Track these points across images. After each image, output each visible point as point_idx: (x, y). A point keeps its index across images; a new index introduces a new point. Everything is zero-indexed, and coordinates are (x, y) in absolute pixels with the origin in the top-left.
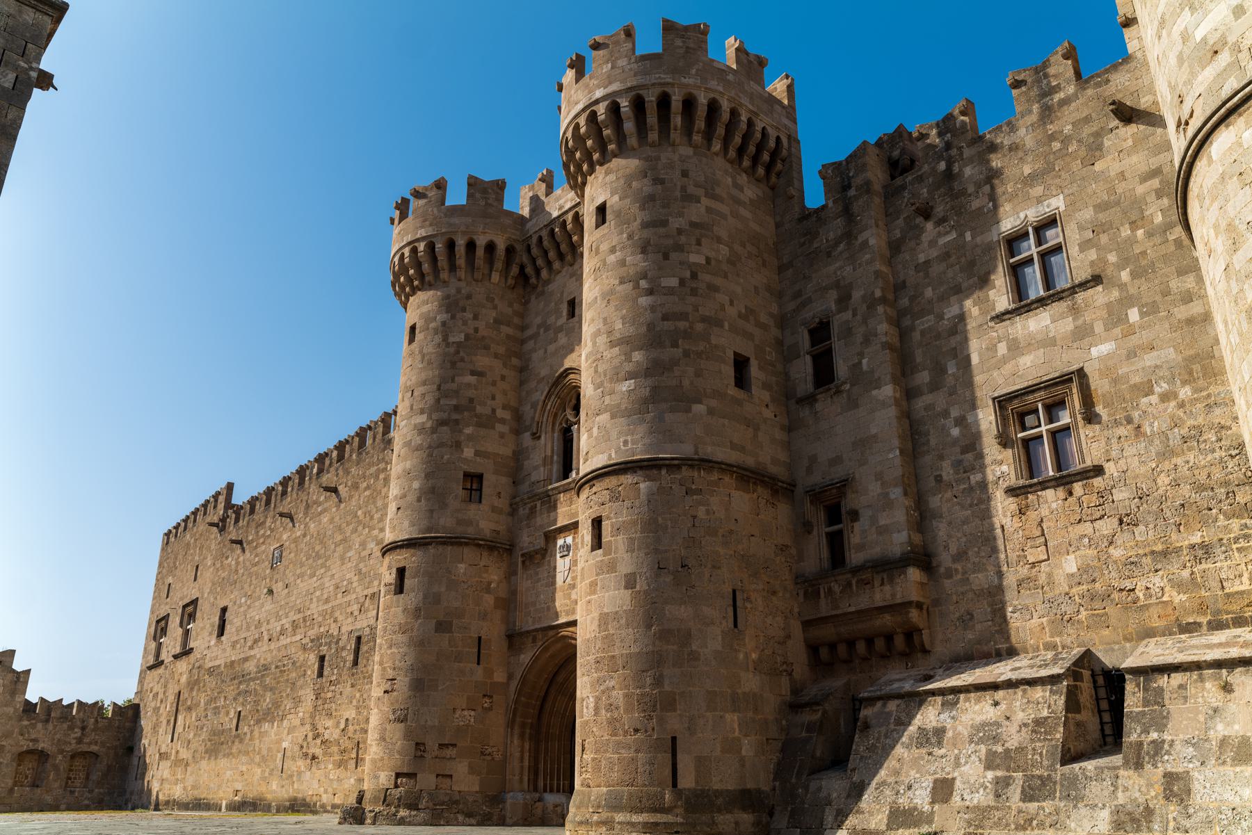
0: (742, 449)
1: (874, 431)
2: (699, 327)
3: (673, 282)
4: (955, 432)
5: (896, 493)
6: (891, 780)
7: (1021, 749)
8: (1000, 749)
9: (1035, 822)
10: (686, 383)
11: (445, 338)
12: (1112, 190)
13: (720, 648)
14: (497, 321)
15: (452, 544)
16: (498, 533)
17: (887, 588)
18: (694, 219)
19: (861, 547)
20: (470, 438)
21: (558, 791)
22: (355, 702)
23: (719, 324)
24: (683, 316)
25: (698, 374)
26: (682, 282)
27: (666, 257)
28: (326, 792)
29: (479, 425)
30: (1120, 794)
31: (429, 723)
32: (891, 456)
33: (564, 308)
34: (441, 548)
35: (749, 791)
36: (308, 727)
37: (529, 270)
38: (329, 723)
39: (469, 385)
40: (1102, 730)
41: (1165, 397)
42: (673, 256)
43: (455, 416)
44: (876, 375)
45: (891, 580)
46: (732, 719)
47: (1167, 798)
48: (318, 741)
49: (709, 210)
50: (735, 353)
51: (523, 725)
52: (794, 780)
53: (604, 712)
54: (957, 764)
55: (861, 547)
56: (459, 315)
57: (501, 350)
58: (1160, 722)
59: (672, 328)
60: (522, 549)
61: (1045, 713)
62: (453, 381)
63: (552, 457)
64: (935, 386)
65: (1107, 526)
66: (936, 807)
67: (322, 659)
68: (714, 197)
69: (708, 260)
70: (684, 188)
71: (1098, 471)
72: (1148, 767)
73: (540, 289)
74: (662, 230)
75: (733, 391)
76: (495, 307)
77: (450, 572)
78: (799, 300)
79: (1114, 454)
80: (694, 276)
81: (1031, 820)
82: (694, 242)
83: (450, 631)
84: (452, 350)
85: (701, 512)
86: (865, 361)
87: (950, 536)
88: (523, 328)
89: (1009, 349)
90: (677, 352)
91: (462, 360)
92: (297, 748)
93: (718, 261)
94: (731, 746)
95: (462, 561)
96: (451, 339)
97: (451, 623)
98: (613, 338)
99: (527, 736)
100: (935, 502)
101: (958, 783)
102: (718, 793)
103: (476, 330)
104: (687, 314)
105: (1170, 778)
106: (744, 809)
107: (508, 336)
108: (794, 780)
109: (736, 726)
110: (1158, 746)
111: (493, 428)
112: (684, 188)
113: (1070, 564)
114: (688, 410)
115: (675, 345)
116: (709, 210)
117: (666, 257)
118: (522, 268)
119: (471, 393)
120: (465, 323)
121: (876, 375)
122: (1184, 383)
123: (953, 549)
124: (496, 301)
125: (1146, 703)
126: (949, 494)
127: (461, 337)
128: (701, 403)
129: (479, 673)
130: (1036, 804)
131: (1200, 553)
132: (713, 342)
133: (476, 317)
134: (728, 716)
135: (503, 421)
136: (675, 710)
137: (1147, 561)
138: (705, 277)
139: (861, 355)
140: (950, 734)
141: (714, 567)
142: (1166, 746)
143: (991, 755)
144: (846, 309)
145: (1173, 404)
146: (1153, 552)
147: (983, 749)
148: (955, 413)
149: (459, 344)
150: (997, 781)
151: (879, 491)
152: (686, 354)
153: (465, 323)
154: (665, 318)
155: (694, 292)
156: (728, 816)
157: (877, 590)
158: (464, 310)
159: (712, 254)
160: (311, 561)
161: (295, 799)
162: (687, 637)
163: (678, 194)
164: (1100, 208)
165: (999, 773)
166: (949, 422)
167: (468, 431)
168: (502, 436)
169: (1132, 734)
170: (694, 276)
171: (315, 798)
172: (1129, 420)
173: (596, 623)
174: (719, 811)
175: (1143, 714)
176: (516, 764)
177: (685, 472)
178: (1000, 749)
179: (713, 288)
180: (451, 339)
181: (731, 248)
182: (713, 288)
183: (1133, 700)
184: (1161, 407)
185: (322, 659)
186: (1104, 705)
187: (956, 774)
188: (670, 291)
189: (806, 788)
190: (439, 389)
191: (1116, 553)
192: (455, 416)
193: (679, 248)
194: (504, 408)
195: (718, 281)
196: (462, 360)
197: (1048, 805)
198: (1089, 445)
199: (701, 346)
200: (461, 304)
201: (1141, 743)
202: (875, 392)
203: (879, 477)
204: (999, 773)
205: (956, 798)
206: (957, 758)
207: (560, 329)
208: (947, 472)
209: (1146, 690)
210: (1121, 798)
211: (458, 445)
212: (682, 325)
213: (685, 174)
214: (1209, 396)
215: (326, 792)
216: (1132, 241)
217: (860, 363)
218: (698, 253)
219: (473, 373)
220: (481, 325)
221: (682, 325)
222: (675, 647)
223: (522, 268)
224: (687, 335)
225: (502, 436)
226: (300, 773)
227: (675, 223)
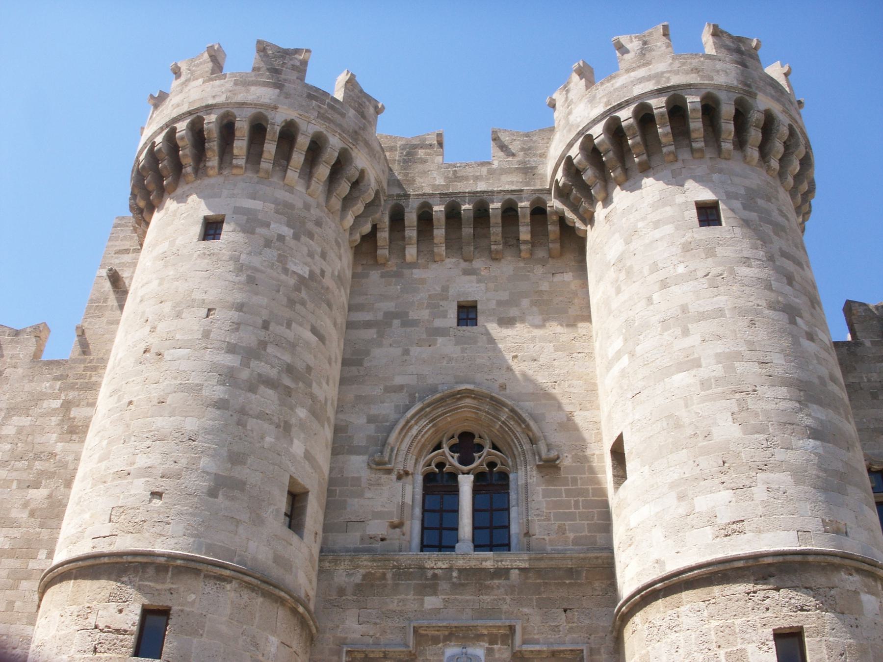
15: (265, 594)
34: (246, 595)
37: (383, 236)
43: (287, 381)
60: (343, 642)
62: (289, 326)
63: (413, 507)
77: (256, 645)
84: (292, 281)
91: (303, 303)
95: (274, 632)
127: (305, 272)
149: (302, 280)
153: (311, 255)
180: (292, 267)
190: (266, 326)
192: (287, 381)
207: (443, 332)
211: (286, 428)
219: (314, 331)
223: (375, 228)
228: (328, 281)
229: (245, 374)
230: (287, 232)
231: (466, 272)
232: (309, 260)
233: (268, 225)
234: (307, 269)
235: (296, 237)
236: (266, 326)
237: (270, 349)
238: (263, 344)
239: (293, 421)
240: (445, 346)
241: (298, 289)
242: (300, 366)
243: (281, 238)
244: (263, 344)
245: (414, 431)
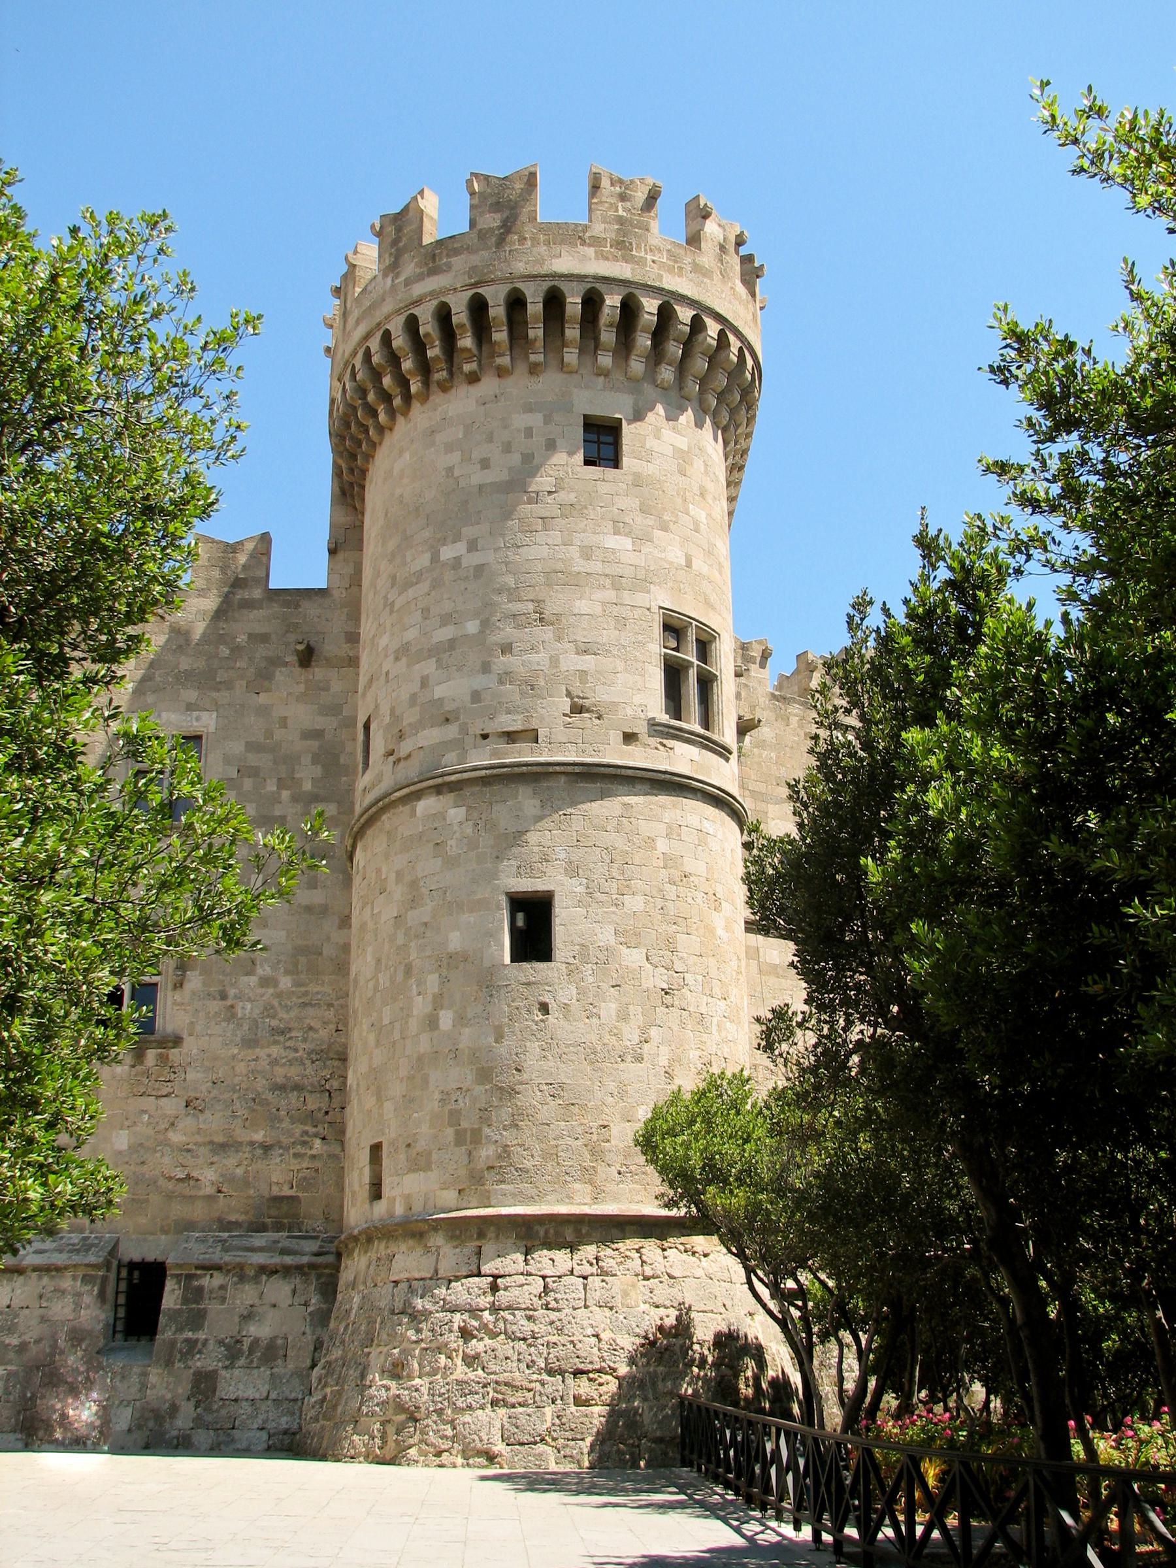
12: (269, 734)
40: (114, 1326)
41: (265, 982)
58: (197, 1320)
65: (171, 1106)
71: (177, 1041)
79: (198, 1028)
110: (191, 1344)
113: (122, 1140)
122: (287, 972)
125: (185, 1300)
131: (259, 1152)
137: (204, 1151)
142: (199, 1345)
145: (271, 991)
146: (211, 1142)
164: (251, 747)
169: (166, 1332)
172: (223, 996)
183: (171, 1297)
184: (261, 991)
186: (122, 1300)
191: (176, 1137)
198: (172, 1012)
209: (186, 1288)
214: (306, 993)
216: (275, 799)
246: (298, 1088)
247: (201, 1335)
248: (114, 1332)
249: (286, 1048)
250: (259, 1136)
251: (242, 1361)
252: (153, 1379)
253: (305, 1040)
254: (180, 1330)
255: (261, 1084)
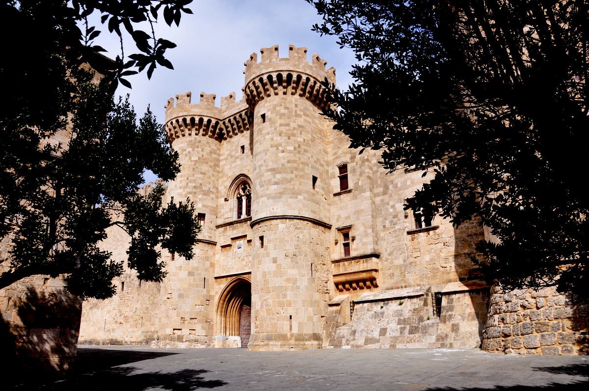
0: (314, 212)
1: (362, 208)
2: (301, 166)
3: (292, 148)
4: (391, 210)
5: (370, 231)
6: (366, 329)
7: (409, 318)
8: (402, 318)
9: (412, 341)
10: (296, 187)
11: (190, 158)
13: (307, 285)
14: (211, 152)
16: (211, 237)
17: (365, 264)
18: (299, 124)
19: (356, 250)
20: (200, 199)
21: (235, 335)
22: (139, 301)
23: (307, 165)
24: (295, 161)
25: (300, 184)
26: (295, 148)
27: (289, 138)
28: (127, 336)
29: (204, 194)
30: (439, 331)
31: (186, 310)
32: (368, 217)
33: (240, 149)
35: (316, 334)
36: (117, 311)
37: (224, 131)
38: (128, 309)
39: (199, 178)
42: (291, 138)
43: (194, 190)
44: (364, 188)
45: (367, 262)
46: (310, 309)
47: (452, 331)
48: (122, 317)
49: (305, 121)
50: (313, 176)
51: (221, 312)
52: (330, 330)
53: (265, 307)
54: (388, 323)
55: (356, 250)
56: (195, 149)
57: (212, 164)
58: (451, 308)
59: (291, 166)
61: (417, 307)
62: (193, 176)
64: (384, 193)
66: (381, 337)
67: (123, 283)
68: (307, 116)
69: (304, 140)
70: (296, 111)
72: (447, 322)
73: (228, 139)
74: (287, 128)
75: (312, 190)
76: (210, 147)
78: (336, 156)
80: (299, 146)
81: (411, 340)
82: (299, 133)
83: (194, 276)
84: (193, 163)
85: (301, 236)
86: (360, 182)
87: (387, 247)
88: (219, 155)
89: (411, 183)
90: (293, 176)
91: (197, 168)
92: (111, 319)
93: (308, 140)
94: (310, 319)
96: (193, 159)
97: (194, 273)
98: (268, 168)
99: (223, 315)
100: (382, 234)
101: (388, 330)
102: (306, 335)
103: (203, 156)
104: (297, 161)
105: (453, 325)
106: (314, 340)
107: (215, 158)
108: (330, 330)
109: (312, 312)
110: (451, 316)
111: (209, 196)
112: (296, 111)
113: (427, 258)
114: (297, 198)
115: (292, 173)
116: (305, 121)
117: (289, 138)
118: (221, 129)
119: (201, 181)
120: (198, 152)
121: (364, 188)
123: (388, 251)
124: (210, 144)
125: (448, 303)
126: (388, 232)
127: (196, 158)
128: (301, 195)
129: (205, 291)
130: (413, 335)
131: (467, 256)
132: (306, 172)
133: (202, 150)
134: (309, 309)
135: (213, 193)
136: (291, 306)
138: (303, 147)
139: (359, 179)
140: (386, 314)
141: (305, 256)
142: (453, 316)
143: (399, 320)
144: (354, 162)
147: (397, 318)
148: (391, 203)
149: (196, 161)
150: (401, 328)
151: (364, 230)
152: (296, 176)
153: (198, 152)
154: (288, 162)
155: (299, 153)
156: (309, 342)
157: (361, 265)
158: (198, 147)
159: (306, 138)
160: (115, 242)
161: (112, 340)
162: (295, 281)
163: (294, 114)
165: (402, 326)
166: (389, 207)
167: (200, 196)
168: (212, 199)
170: (299, 146)
171: (122, 339)
173: (261, 275)
174: (306, 340)
175: (447, 306)
176: (218, 325)
177: (295, 221)
178: (402, 318)
179: (306, 151)
180: (193, 159)
181: (312, 136)
182: (306, 151)
185: (123, 283)
187: (387, 327)
188: (290, 152)
189: (335, 332)
190: (188, 179)
192: (194, 190)
193: (294, 135)
194: (214, 187)
195: (307, 148)
196: (197, 168)
197: (417, 335)
199: (301, 173)
200: (197, 144)
201: (446, 316)
202: (363, 194)
203: (364, 225)
204: (402, 326)
205: (387, 334)
206: (388, 321)
207: (237, 158)
208: (388, 224)
210: (439, 332)
212: (295, 165)
213: (296, 106)
215: (127, 336)
217: (358, 183)
218: (301, 137)
219: (201, 173)
220: (205, 154)
221: (295, 165)
222: (292, 284)
224: (296, 169)
225: (212, 199)
226: (113, 330)
227: (293, 125)
228: (205, 156)
229: (184, 193)
230: (190, 149)
231: (243, 136)
232: (198, 154)
233: (186, 150)
234: (197, 158)
235: (193, 150)
236: (188, 179)
237: (189, 184)
238: (187, 184)
239: (197, 200)
240: (238, 162)
241: (195, 165)
242: (198, 185)
243: (189, 152)
244: (187, 184)
245: (232, 188)
246: (476, 234)
247: (453, 313)
248: (434, 314)
249: (470, 223)
250: (466, 251)
251: (466, 320)
252: (440, 327)
253: (475, 220)
254: (447, 312)
255: (464, 235)
